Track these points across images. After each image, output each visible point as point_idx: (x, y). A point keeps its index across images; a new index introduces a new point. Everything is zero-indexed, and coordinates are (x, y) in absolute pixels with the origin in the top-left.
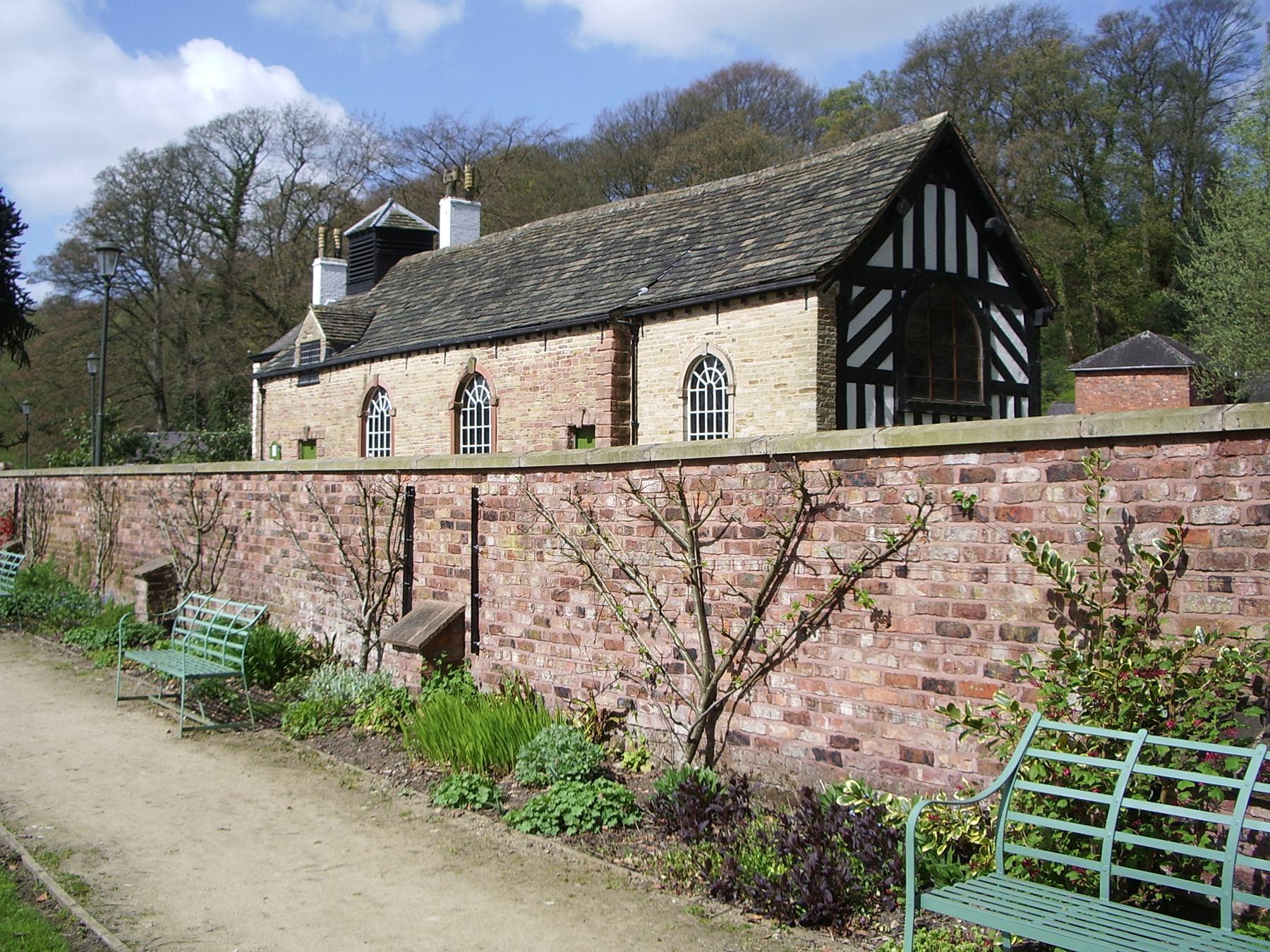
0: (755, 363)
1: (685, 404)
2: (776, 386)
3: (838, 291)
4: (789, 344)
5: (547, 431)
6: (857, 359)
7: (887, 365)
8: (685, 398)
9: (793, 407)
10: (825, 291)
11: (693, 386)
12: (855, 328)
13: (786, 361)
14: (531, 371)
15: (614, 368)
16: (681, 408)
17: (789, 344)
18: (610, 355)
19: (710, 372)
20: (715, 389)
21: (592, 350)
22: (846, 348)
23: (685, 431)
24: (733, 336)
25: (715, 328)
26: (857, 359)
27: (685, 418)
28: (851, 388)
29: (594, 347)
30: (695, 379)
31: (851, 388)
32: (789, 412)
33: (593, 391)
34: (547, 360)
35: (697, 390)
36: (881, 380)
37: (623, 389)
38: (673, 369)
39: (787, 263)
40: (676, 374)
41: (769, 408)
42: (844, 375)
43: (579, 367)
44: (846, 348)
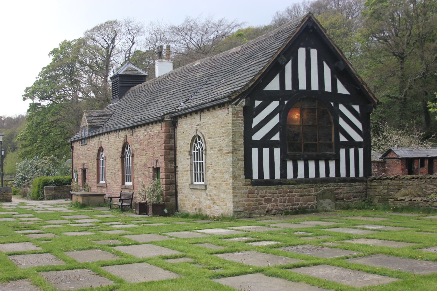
0: (212, 139)
1: (191, 158)
2: (219, 150)
3: (244, 104)
4: (222, 130)
5: (147, 169)
6: (258, 136)
7: (276, 137)
8: (191, 155)
9: (225, 161)
10: (236, 104)
11: (194, 150)
12: (256, 121)
13: (222, 138)
14: (142, 142)
15: (165, 141)
16: (189, 159)
17: (222, 130)
18: (163, 135)
19: (199, 143)
20: (201, 151)
21: (159, 133)
22: (249, 131)
23: (191, 171)
24: (205, 126)
25: (199, 123)
26: (258, 136)
27: (191, 164)
28: (255, 151)
29: (158, 130)
30: (195, 146)
31: (255, 151)
32: (224, 163)
33: (159, 151)
34: (147, 137)
35: (196, 151)
36: (272, 145)
37: (171, 149)
38: (186, 141)
39: (223, 91)
40: (188, 144)
41: (217, 160)
42: (249, 144)
43: (155, 141)
44: (249, 131)
